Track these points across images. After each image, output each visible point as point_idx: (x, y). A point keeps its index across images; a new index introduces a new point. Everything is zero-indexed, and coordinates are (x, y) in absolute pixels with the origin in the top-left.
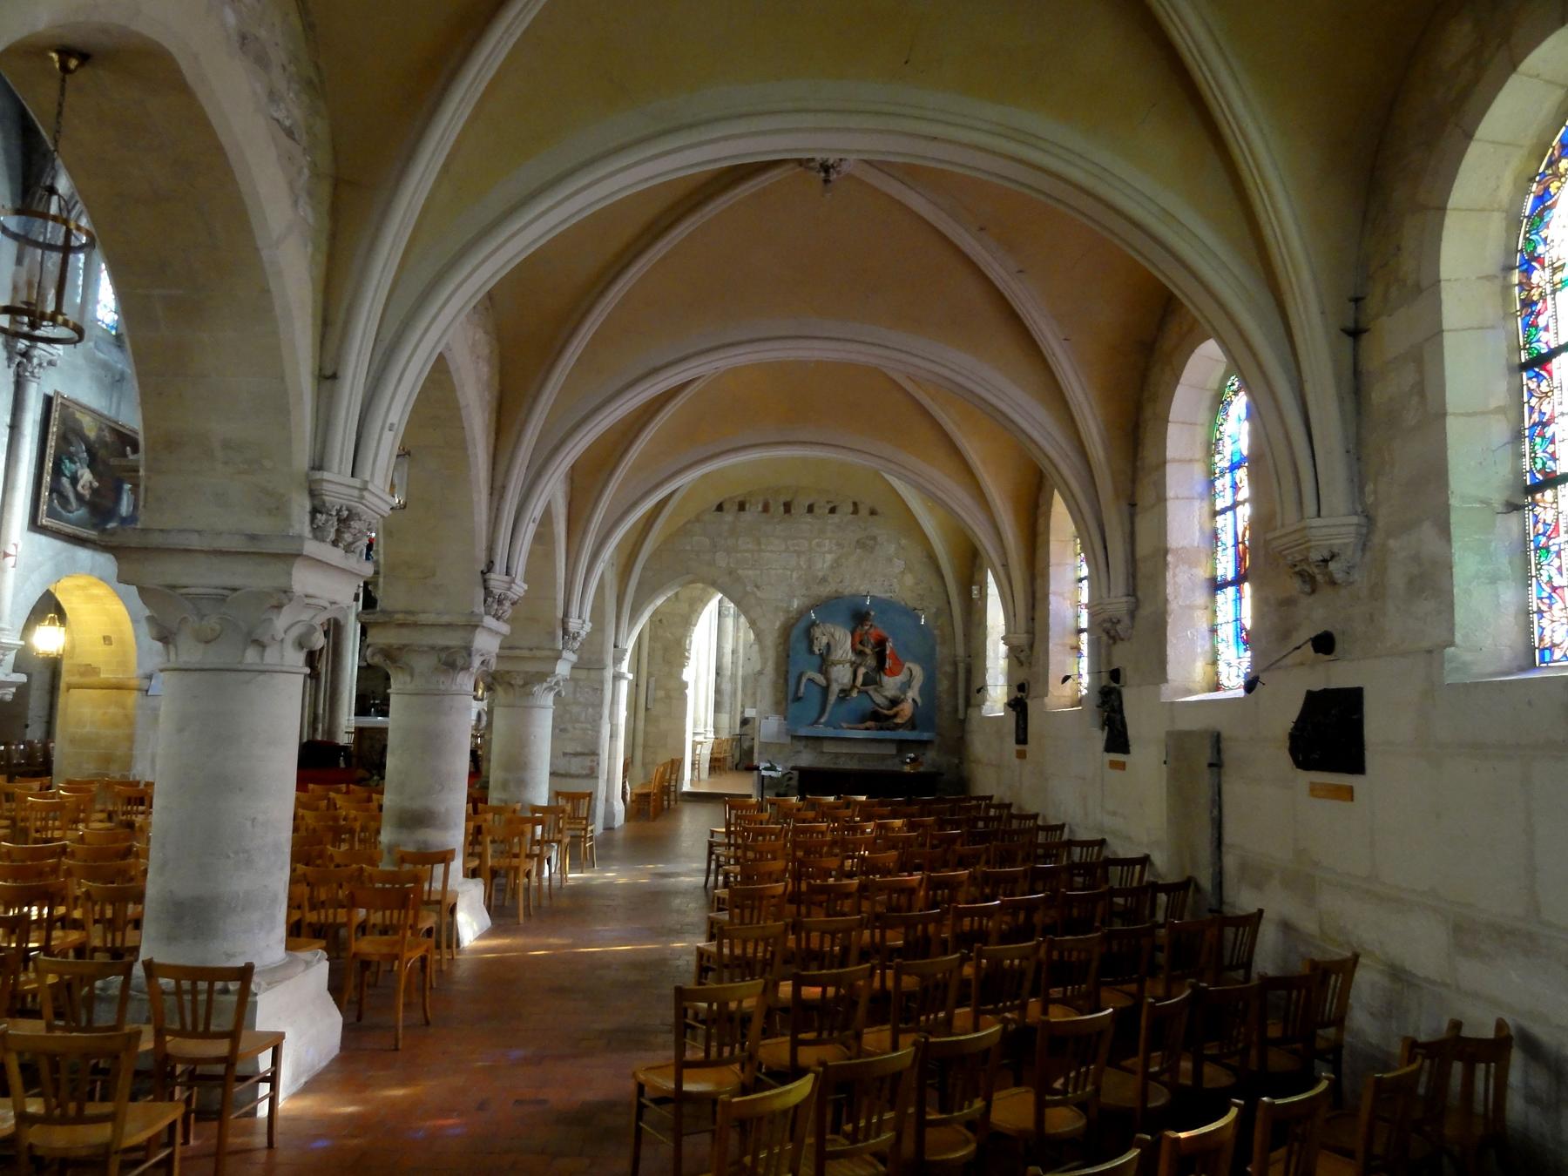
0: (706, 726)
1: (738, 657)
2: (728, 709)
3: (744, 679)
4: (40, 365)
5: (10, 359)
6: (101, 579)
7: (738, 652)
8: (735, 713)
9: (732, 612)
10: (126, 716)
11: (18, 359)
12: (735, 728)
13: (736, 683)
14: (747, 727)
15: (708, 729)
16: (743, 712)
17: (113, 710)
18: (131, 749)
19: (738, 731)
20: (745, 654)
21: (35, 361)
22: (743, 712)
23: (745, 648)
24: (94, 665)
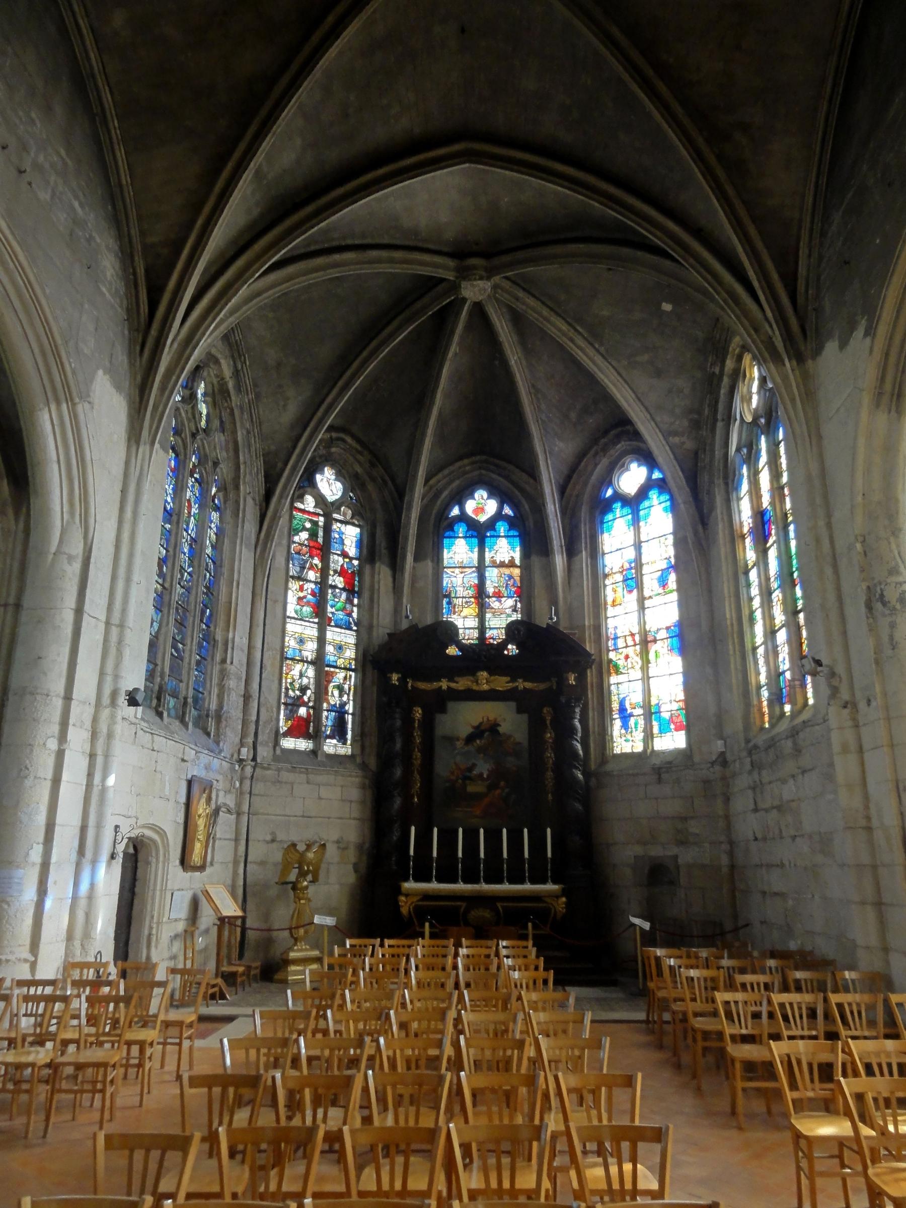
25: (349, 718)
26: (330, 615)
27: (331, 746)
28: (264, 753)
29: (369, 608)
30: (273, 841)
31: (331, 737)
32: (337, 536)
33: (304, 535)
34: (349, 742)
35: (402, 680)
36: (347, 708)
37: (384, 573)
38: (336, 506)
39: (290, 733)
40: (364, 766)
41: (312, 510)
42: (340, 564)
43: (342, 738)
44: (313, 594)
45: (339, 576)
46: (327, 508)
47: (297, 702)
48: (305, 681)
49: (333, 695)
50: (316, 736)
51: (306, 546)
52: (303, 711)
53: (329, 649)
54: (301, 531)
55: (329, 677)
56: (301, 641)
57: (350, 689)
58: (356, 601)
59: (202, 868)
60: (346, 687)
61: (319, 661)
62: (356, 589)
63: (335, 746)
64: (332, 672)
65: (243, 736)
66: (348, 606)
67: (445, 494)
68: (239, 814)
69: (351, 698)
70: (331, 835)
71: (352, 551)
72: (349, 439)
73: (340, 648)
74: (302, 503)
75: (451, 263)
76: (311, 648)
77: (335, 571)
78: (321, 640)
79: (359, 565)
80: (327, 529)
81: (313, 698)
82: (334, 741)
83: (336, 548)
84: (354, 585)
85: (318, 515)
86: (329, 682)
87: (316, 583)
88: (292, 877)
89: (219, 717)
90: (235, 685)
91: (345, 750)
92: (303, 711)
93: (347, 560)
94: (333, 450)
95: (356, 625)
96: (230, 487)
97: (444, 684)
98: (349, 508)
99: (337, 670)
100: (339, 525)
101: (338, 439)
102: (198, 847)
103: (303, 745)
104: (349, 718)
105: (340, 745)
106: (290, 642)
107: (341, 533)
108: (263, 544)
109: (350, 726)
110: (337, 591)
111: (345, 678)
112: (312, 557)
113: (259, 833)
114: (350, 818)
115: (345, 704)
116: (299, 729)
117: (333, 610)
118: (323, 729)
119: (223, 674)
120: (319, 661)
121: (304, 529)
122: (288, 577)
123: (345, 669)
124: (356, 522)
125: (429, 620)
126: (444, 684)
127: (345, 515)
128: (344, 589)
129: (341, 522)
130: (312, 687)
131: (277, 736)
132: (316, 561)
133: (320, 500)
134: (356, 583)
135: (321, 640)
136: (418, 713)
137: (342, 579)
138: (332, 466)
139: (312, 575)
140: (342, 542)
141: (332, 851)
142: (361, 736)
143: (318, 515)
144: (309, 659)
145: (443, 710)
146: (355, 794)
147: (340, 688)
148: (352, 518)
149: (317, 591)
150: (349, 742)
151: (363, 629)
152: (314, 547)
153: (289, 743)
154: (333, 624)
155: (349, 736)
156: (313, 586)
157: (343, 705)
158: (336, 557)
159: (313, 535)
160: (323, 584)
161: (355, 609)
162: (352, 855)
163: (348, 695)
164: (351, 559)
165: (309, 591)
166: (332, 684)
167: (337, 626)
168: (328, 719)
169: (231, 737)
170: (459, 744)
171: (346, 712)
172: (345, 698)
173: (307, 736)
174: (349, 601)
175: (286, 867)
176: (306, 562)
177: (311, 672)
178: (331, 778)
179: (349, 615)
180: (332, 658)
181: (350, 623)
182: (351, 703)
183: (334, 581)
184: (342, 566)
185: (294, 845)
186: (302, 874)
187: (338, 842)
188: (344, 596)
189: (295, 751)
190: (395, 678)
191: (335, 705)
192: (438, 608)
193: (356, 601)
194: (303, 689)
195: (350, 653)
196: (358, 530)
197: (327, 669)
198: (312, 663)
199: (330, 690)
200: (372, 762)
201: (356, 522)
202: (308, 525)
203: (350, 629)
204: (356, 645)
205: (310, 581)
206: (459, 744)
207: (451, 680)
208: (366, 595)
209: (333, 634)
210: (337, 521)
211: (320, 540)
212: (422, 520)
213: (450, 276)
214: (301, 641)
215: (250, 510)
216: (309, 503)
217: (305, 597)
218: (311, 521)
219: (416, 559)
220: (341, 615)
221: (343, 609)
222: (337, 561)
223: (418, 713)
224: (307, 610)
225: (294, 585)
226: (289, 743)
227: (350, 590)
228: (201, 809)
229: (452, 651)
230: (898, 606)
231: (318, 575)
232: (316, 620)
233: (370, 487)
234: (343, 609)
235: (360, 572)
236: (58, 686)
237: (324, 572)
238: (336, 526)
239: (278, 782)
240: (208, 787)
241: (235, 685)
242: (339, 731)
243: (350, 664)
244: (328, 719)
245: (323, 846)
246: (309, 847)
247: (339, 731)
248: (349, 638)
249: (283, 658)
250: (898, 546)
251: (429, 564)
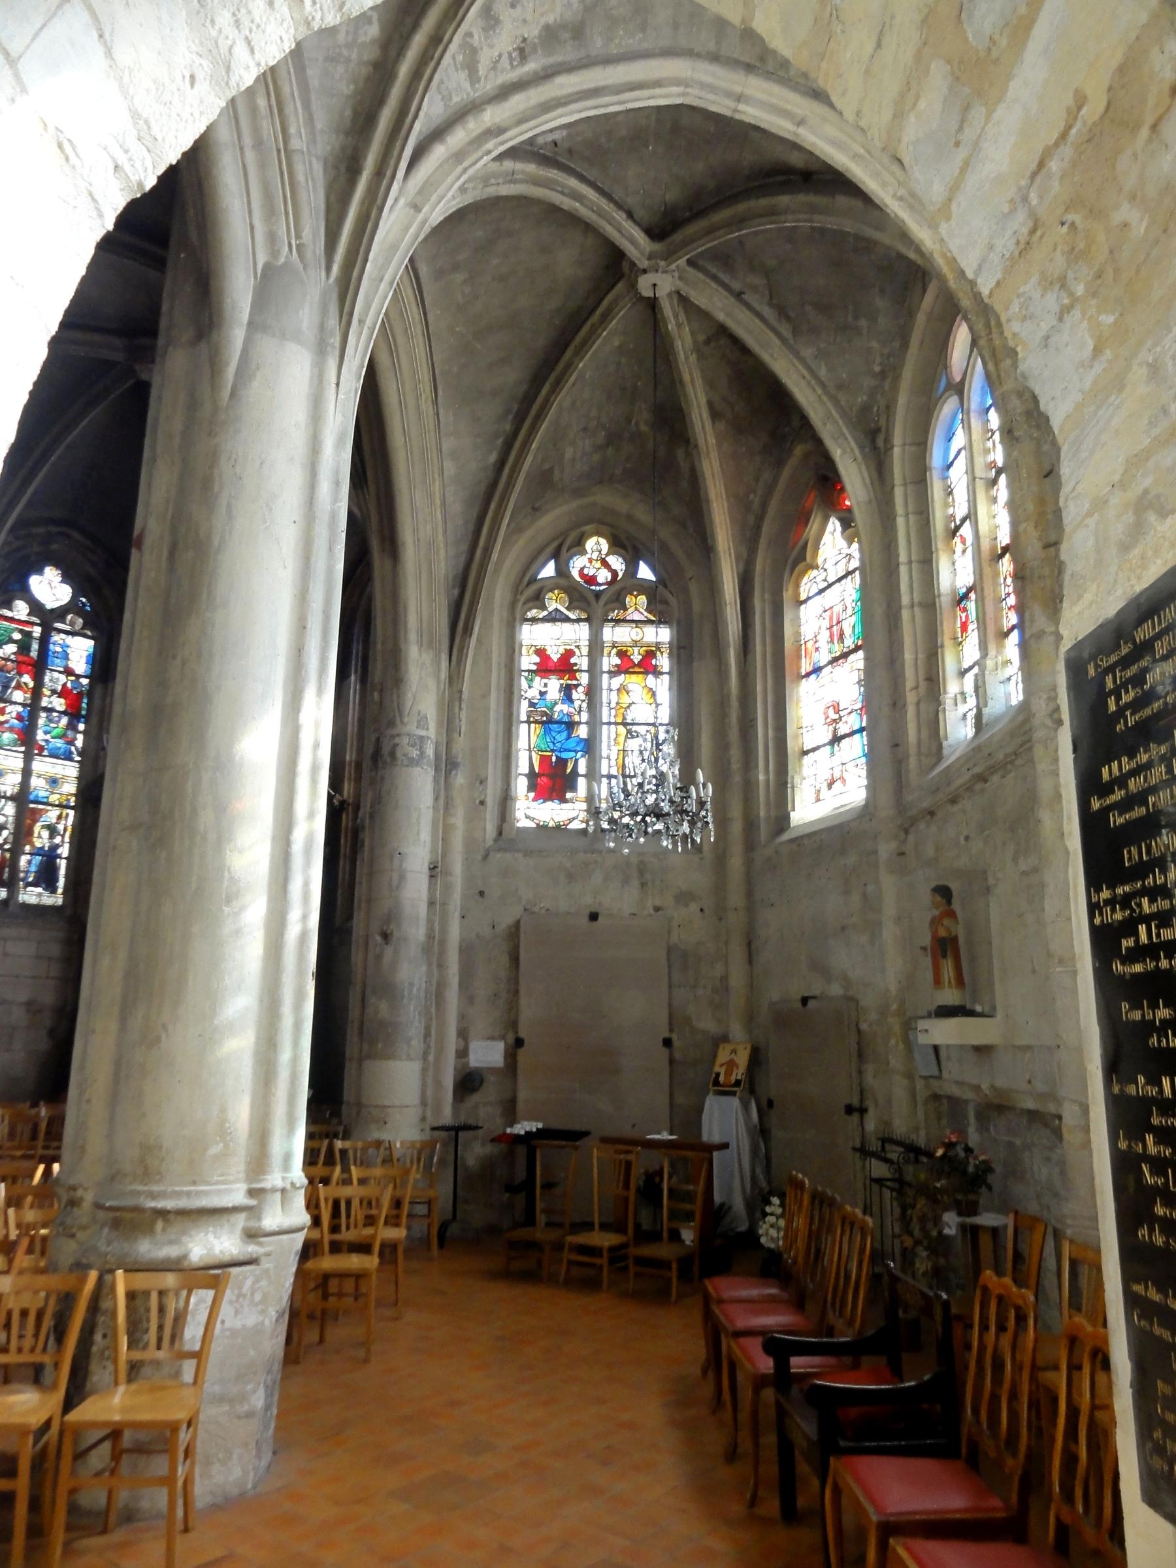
0: (259, 1163)
1: (448, 888)
2: (417, 1045)
3: (466, 951)
7: (447, 873)
8: (440, 1051)
9: (430, 751)
12: (438, 1110)
13: (441, 966)
14: (475, 1098)
15: (275, 1179)
16: (462, 1053)
19: (447, 1116)
20: (469, 879)
22: (462, 1053)
23: (468, 862)
25: (63, 864)
26: (43, 743)
31: (35, 884)
32: (58, 649)
34: (60, 891)
36: (59, 851)
38: (60, 613)
41: (24, 618)
42: (61, 683)
43: (51, 887)
44: (19, 717)
45: (59, 697)
46: (48, 618)
49: (40, 837)
51: (12, 661)
53: (34, 782)
54: (6, 643)
55: (35, 815)
57: (65, 830)
58: (81, 727)
60: (61, 827)
62: (83, 713)
63: (40, 895)
64: (41, 810)
66: (70, 733)
69: (67, 839)
71: (80, 666)
72: (76, 535)
73: (54, 782)
74: (10, 609)
75: (118, 342)
77: (54, 692)
78: (27, 773)
79: (90, 684)
80: (44, 640)
81: (11, 839)
82: (40, 890)
83: (57, 664)
84: (80, 708)
85: (33, 624)
86: (35, 821)
87: (24, 705)
91: (49, 900)
93: (73, 678)
94: (55, 547)
95: (79, 754)
98: (80, 616)
99: (49, 808)
100: (63, 636)
101: (61, 534)
104: (63, 864)
105: (46, 893)
107: (65, 646)
109: (62, 872)
110: (55, 714)
111: (60, 817)
112: (20, 674)
114: (47, 977)
115: (57, 846)
117: (48, 737)
118: (22, 875)
121: (11, 641)
123: (61, 806)
124: (89, 633)
127: (72, 624)
128: (64, 713)
129: (67, 633)
130: (11, 826)
132: (27, 679)
133: (36, 607)
134: (84, 705)
135: (27, 773)
137: (62, 701)
138: (57, 566)
140: (66, 656)
143: (33, 624)
144: (8, 794)
147: (52, 830)
148: (83, 628)
149: (25, 714)
150: (60, 891)
152: (24, 663)
154: (46, 753)
155: (61, 883)
156: (20, 709)
158: (56, 675)
159: (24, 647)
160: (34, 706)
161: (80, 737)
163: (63, 836)
164: (78, 677)
165: (14, 715)
166: (39, 824)
167: (51, 756)
171: (59, 857)
172: (58, 840)
174: (72, 726)
176: (11, 679)
179: (71, 742)
180: (42, 794)
181: (71, 753)
182: (67, 846)
183: (51, 703)
184: (64, 685)
187: (29, 1004)
188: (65, 720)
191: (42, 848)
193: (81, 727)
195: (70, 788)
196: (91, 643)
197: (32, 806)
198: (11, 798)
199: (37, 828)
201: (89, 633)
202: (17, 636)
203: (71, 760)
204: (79, 778)
205: (15, 703)
208: (94, 720)
210: (60, 631)
211: (34, 654)
213: (119, 356)
216: (21, 609)
217: (6, 722)
218: (21, 631)
220: (59, 743)
221: (62, 736)
222: (54, 679)
227: (73, 714)
230: (388, 760)
231: (28, 695)
232: (23, 749)
234: (62, 736)
235: (90, 693)
237: (37, 693)
238: (57, 638)
242: (46, 877)
243: (68, 800)
250: (399, 697)
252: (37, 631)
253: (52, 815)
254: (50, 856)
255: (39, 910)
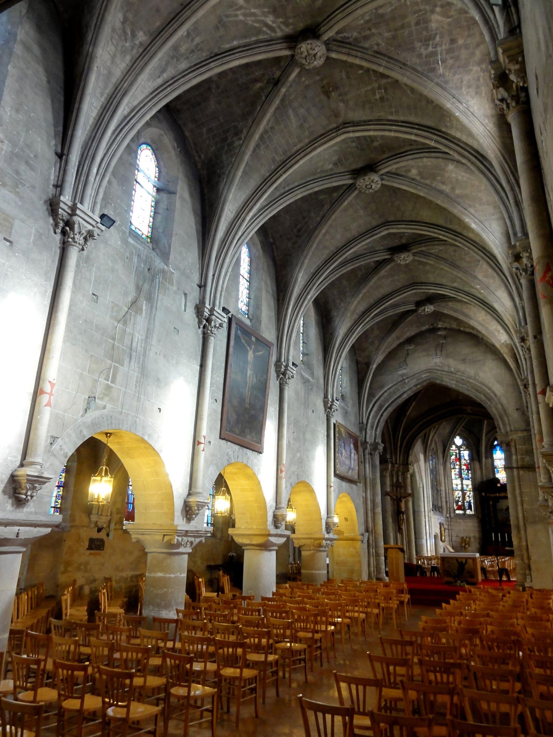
4: (334, 411)
5: (325, 410)
6: (348, 494)
10: (357, 553)
11: (328, 410)
17: (351, 549)
18: (361, 567)
21: (333, 410)
24: (342, 530)
25: (472, 504)
27: (468, 512)
28: (452, 515)
29: (474, 474)
30: (457, 536)
33: (453, 457)
35: (486, 494)
37: (477, 465)
38: (461, 447)
39: (458, 509)
40: (478, 517)
43: (471, 510)
46: (459, 448)
47: (458, 501)
48: (459, 496)
50: (464, 510)
52: (460, 503)
53: (465, 486)
55: (466, 493)
56: (457, 485)
59: (444, 542)
61: (462, 490)
65: (447, 511)
67: (492, 439)
68: (449, 530)
70: (472, 535)
71: (467, 458)
76: (459, 487)
78: (462, 484)
80: (460, 454)
83: (462, 459)
88: (463, 545)
89: (442, 507)
90: (444, 500)
91: (472, 513)
92: (460, 503)
96: (436, 453)
97: (498, 495)
102: (443, 538)
103: (461, 512)
106: (454, 486)
108: (445, 463)
113: (454, 535)
116: (459, 508)
119: (441, 498)
120: (462, 490)
122: (451, 469)
125: (492, 477)
126: (498, 495)
131: (454, 510)
132: (458, 463)
133: (457, 446)
135: (462, 484)
136: (491, 503)
139: (457, 467)
140: (464, 456)
141: (472, 539)
142: (476, 510)
145: (498, 502)
146: (476, 524)
147: (469, 496)
151: (473, 479)
153: (457, 512)
157: (470, 501)
159: (456, 456)
160: (461, 469)
162: (478, 541)
168: (466, 505)
169: (445, 512)
170: (504, 511)
173: (462, 510)
174: (468, 472)
175: (462, 542)
177: (460, 493)
178: (470, 521)
185: (463, 537)
186: (466, 544)
187: (474, 537)
189: (459, 514)
190: (483, 494)
192: (494, 474)
194: (459, 498)
195: (470, 487)
200: (480, 516)
203: (469, 479)
206: (504, 511)
207: (499, 493)
209: (465, 482)
212: (486, 447)
214: (457, 485)
215: (441, 455)
216: (454, 447)
219: (486, 458)
220: (466, 476)
222: (463, 462)
223: (491, 503)
224: (457, 476)
225: (453, 471)
226: (457, 512)
227: (468, 469)
228: (443, 529)
229: (499, 485)
233: (470, 440)
235: (470, 464)
236: (423, 510)
238: (461, 452)
239: (456, 522)
240: (443, 524)
241: (444, 500)
242: (470, 508)
244: (466, 505)
245: (470, 538)
246: (467, 538)
247: (470, 508)
248: (469, 482)
249: (453, 490)
251: (490, 460)
252: (457, 451)
253: (468, 493)
254: (469, 503)
255: (470, 516)
